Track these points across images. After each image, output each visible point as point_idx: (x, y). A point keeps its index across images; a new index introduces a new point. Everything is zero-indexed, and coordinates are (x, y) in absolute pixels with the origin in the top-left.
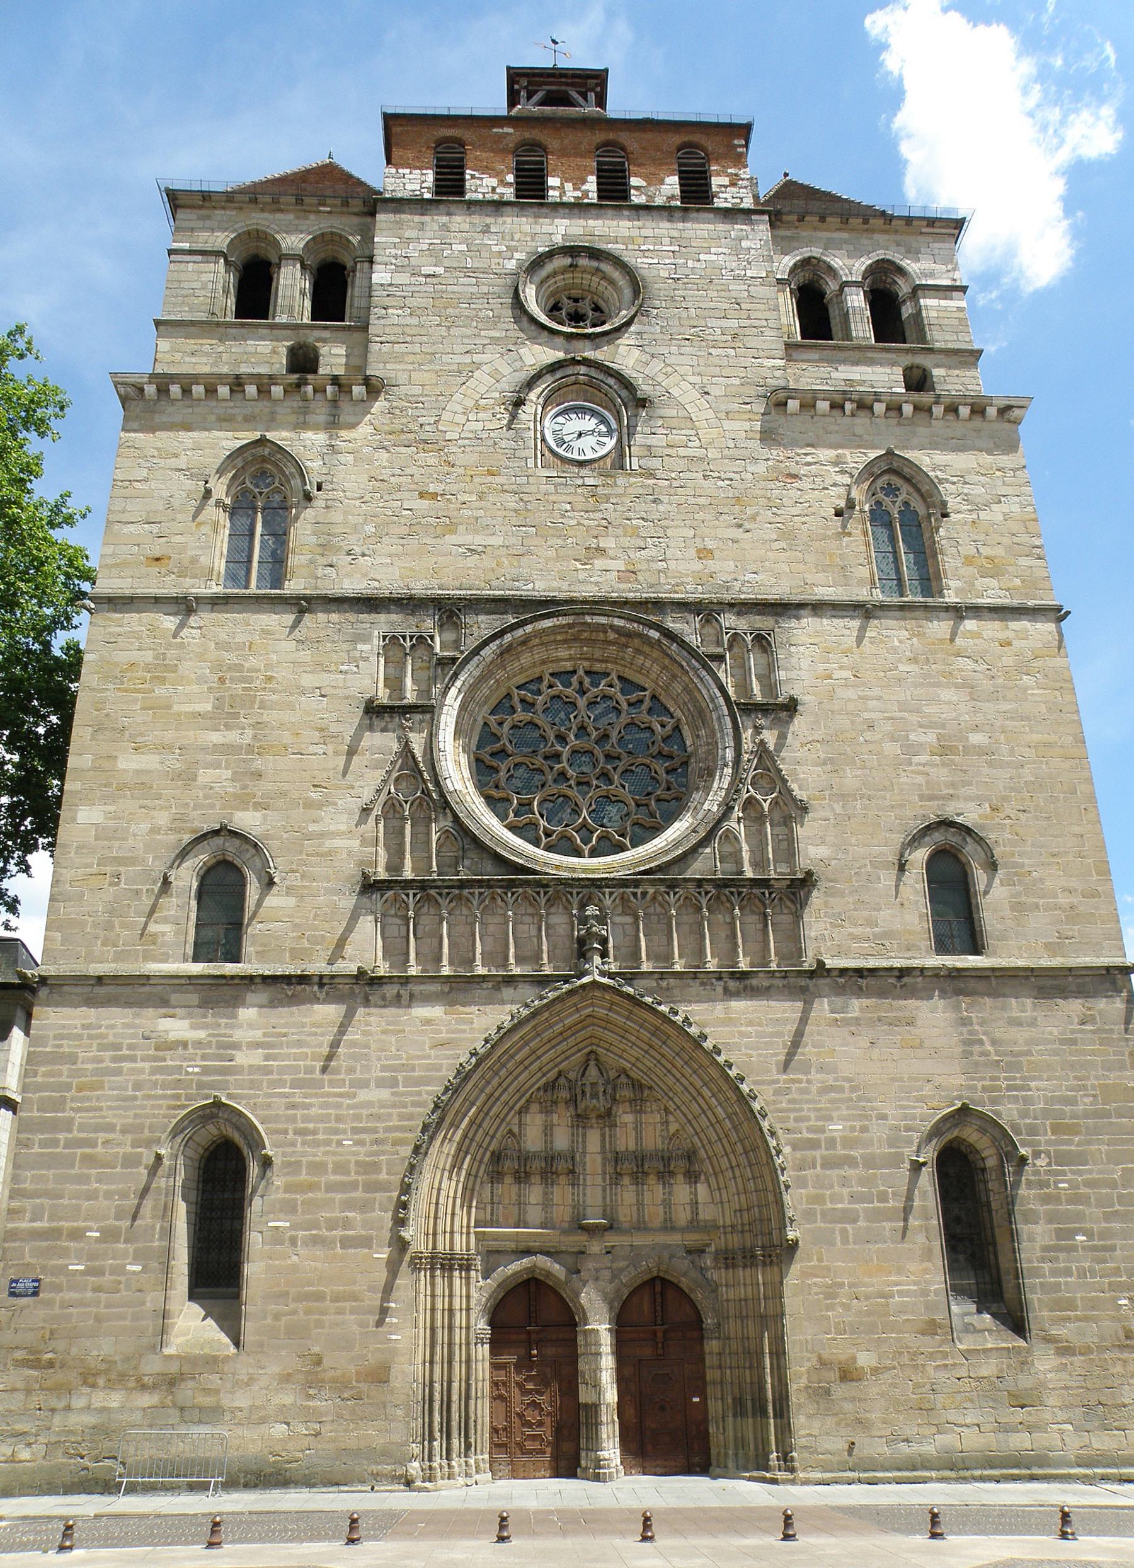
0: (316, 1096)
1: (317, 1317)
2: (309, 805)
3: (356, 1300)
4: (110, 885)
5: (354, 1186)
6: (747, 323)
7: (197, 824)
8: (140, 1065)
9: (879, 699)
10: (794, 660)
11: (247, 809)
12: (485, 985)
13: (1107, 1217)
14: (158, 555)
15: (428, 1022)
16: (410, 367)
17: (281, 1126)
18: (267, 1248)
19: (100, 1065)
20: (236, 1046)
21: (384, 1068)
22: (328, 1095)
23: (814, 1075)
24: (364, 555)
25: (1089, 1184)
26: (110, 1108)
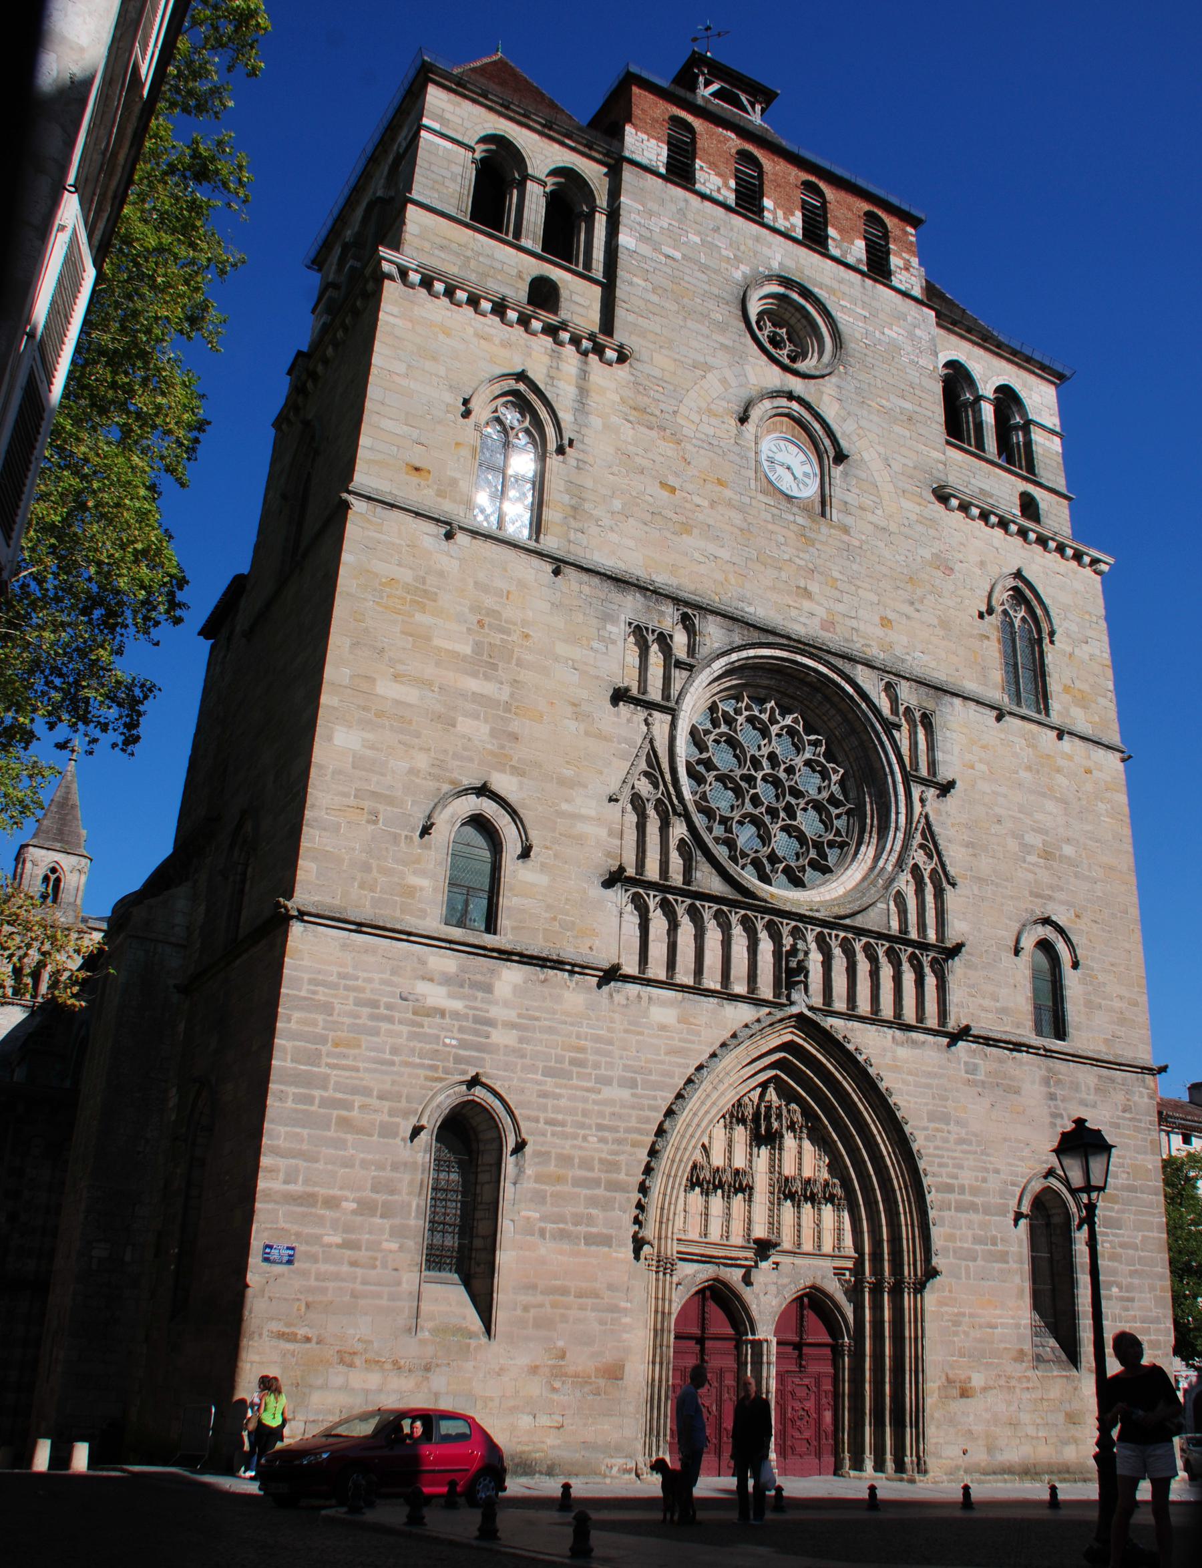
0: (565, 1086)
1: (562, 1311)
2: (562, 782)
3: (597, 1296)
4: (368, 822)
5: (596, 1183)
6: (918, 409)
7: (455, 775)
8: (397, 1027)
9: (1005, 796)
10: (949, 745)
11: (503, 771)
12: (711, 999)
13: (1133, 1273)
14: (418, 465)
15: (663, 1028)
16: (652, 346)
17: (533, 1113)
18: (518, 1237)
19: (358, 1021)
20: (491, 1023)
21: (626, 1068)
22: (577, 1088)
23: (952, 1127)
24: (612, 529)
26: (366, 1070)
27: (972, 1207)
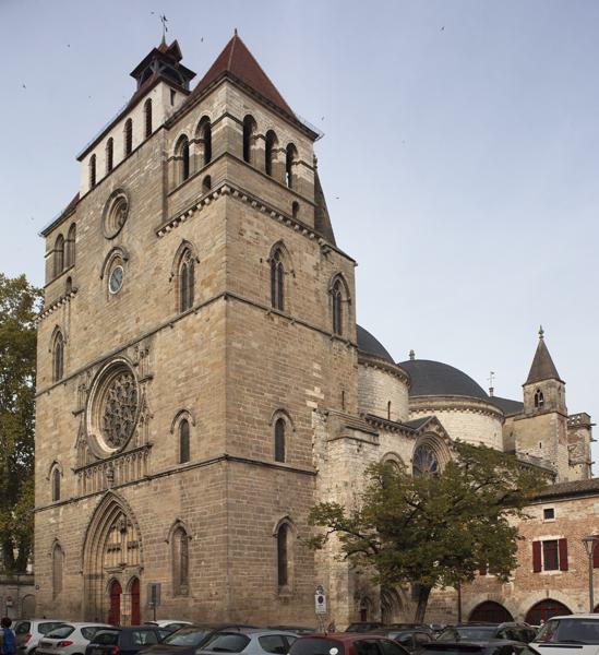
13: (211, 555)
25: (208, 543)
27: (154, 541)
